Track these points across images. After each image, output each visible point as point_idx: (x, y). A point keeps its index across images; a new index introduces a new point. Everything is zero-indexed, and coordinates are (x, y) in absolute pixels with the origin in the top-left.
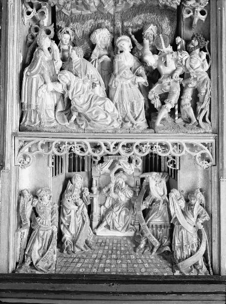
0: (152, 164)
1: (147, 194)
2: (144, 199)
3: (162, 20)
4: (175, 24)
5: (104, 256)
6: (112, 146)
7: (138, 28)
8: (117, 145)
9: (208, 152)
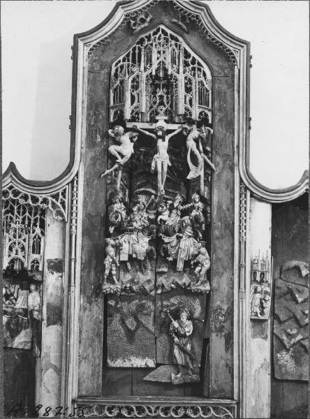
3: (194, 301)
4: (205, 306)
8: (157, 408)
9: (230, 414)
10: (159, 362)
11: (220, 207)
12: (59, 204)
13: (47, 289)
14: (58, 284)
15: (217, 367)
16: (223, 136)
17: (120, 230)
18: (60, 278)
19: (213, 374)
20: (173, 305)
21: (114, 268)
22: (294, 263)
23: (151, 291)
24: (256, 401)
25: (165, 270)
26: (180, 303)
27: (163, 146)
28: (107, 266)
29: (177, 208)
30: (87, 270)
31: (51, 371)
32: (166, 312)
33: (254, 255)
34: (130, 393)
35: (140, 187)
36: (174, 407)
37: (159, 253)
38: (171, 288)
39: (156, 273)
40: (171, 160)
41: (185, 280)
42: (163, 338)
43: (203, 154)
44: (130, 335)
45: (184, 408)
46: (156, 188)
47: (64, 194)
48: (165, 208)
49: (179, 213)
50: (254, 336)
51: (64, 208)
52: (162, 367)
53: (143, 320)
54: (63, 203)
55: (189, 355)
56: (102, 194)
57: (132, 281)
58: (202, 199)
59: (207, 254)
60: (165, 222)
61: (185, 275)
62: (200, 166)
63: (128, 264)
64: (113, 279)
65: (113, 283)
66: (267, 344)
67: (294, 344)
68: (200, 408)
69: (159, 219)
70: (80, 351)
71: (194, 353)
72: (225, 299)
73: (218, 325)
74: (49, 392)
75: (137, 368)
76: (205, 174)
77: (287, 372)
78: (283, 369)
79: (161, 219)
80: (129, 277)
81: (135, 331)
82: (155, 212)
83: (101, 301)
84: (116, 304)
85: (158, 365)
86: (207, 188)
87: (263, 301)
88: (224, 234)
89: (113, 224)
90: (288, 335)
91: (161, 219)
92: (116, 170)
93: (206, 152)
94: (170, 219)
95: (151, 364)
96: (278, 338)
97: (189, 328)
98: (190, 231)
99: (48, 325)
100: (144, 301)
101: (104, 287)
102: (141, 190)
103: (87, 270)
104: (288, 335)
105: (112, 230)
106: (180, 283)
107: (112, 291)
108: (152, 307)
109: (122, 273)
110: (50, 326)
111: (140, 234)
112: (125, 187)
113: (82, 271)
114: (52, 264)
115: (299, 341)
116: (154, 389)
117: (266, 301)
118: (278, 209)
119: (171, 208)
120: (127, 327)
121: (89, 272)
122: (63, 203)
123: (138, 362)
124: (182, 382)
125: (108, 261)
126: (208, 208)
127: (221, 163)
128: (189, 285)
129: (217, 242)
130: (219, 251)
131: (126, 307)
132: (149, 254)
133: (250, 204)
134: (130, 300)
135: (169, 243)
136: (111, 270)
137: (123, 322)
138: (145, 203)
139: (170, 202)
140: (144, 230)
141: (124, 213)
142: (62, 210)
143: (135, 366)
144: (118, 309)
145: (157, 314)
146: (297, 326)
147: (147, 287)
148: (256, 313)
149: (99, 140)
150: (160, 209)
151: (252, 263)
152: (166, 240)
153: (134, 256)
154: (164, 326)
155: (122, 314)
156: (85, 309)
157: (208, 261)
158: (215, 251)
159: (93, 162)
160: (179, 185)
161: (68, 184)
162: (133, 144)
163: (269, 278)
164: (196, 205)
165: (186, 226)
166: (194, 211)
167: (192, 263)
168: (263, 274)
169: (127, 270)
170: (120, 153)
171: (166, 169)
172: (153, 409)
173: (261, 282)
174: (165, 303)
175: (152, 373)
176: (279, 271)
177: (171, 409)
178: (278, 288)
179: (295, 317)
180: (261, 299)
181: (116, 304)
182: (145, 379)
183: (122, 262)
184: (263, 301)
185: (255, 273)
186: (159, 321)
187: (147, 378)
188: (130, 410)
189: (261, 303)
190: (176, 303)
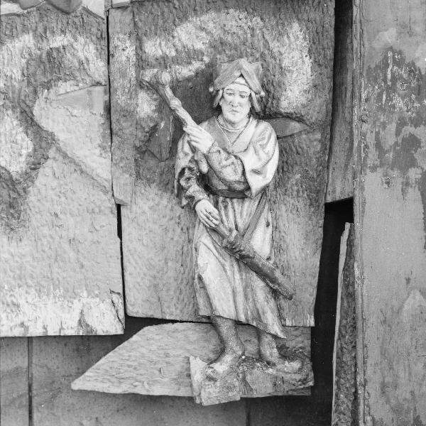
7: (197, 65)
10: (137, 311)
19: (374, 355)
20: (192, 55)
26: (218, 46)
32: (154, 87)
42: (150, 208)
52: (149, 331)
53: (50, 116)
85: (133, 324)
95: (108, 324)
97: (255, 152)
108: (98, 68)
123: (55, 317)
124: (236, 395)
143: (36, 331)
145: (120, 99)
154: (154, 153)
174: (153, 48)
186: (126, 127)
190: (199, 46)
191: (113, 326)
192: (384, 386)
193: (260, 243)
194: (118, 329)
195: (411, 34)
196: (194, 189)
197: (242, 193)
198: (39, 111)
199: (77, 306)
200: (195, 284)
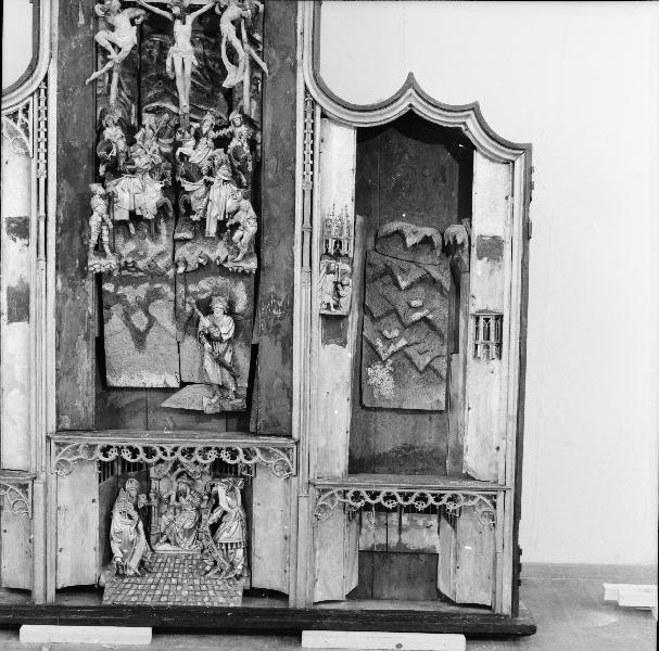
0: (220, 469)
1: (216, 505)
2: (212, 512)
5: (162, 581)
6: (169, 451)
8: (175, 449)
9: (287, 459)
10: (185, 380)
11: (275, 135)
12: (18, 127)
13: (7, 265)
14: (23, 257)
15: (269, 388)
16: (281, 15)
17: (115, 171)
18: (26, 248)
20: (204, 291)
21: (105, 232)
22: (396, 226)
23: (167, 269)
24: (327, 439)
25: (189, 235)
27: (183, 31)
28: (94, 229)
29: (206, 135)
30: (67, 235)
31: (16, 391)
33: (327, 212)
34: (143, 425)
35: (152, 100)
36: (200, 447)
37: (177, 207)
38: (200, 265)
39: (175, 241)
40: (197, 55)
41: (220, 252)
42: (190, 343)
43: (247, 46)
44: (140, 338)
45: (217, 449)
46: (176, 102)
47: (25, 111)
48: (187, 135)
49: (210, 142)
50: (326, 341)
51: (28, 136)
54: (25, 127)
55: (229, 369)
56: (90, 111)
57: (134, 253)
58: (247, 120)
59: (251, 211)
60: (188, 157)
61: (221, 244)
62: (241, 65)
63: (131, 226)
64: (104, 251)
65: (105, 256)
66: (347, 354)
67: (393, 353)
68: (241, 451)
69: (178, 154)
70: (59, 363)
71: (237, 368)
72: (282, 282)
73: (271, 324)
74: (14, 423)
75: (152, 389)
76: (253, 80)
77: (381, 396)
78: (376, 391)
79: (181, 153)
80: (131, 246)
81: (147, 331)
82: (171, 141)
83: (90, 285)
84: (116, 289)
85: (183, 384)
86: (254, 103)
87: (339, 286)
88: (281, 177)
89: (105, 161)
90: (385, 339)
91: (181, 153)
92: (110, 72)
93: (253, 42)
94: (198, 153)
95: (174, 383)
96: (370, 344)
97: (226, 327)
98: (226, 172)
99: (11, 320)
100: (158, 286)
101: (90, 263)
102: (154, 105)
103: (67, 235)
104: (385, 339)
105: (102, 169)
106: (213, 257)
107: (103, 270)
108: (171, 295)
109: (120, 240)
110: (13, 324)
111: (148, 176)
112: (129, 102)
113: (58, 235)
114: (13, 225)
115: (401, 350)
116: (181, 420)
117: (342, 285)
118: (364, 136)
119: (198, 136)
120: (133, 325)
121: (72, 237)
122: (25, 127)
123: (155, 381)
124: (218, 410)
125: (94, 221)
126: (258, 136)
127: (278, 61)
128: (226, 261)
129: (270, 191)
130: (274, 206)
131: (132, 294)
132: (162, 209)
133: (322, 129)
134: (136, 282)
135: (193, 192)
136: (100, 239)
137: (127, 317)
138: (154, 126)
139: (196, 125)
140: (153, 170)
141: (122, 144)
142: (25, 138)
143: (148, 385)
144: (118, 297)
145: (180, 306)
146: (399, 325)
147: (161, 263)
148: (328, 304)
149: (82, 21)
150: (179, 136)
151: (326, 224)
152: (188, 186)
153: (138, 213)
154: (189, 325)
155: (126, 304)
156: (65, 297)
157: (252, 221)
158: (267, 206)
159: (72, 58)
160: (217, 98)
161: (32, 95)
162: (135, 28)
163: (351, 249)
164: (238, 130)
165: (220, 165)
166: (234, 140)
167: (228, 224)
168: (338, 243)
169: (129, 237)
170: (114, 45)
171: (188, 70)
172: (169, 451)
173: (337, 256)
174: (192, 288)
175: (175, 396)
176: (373, 238)
177: (196, 452)
178: (370, 264)
179: (395, 311)
180: (336, 283)
181: (116, 289)
182: (163, 405)
183: (123, 223)
184: (339, 286)
185: (327, 242)
187: (170, 402)
188: (135, 452)
189: (336, 289)
191: (177, 385)
192: (267, 410)
193: (228, 358)
194: (177, 385)
195: (280, 288)
196: (204, 339)
197: (220, 340)
198: (150, 311)
199: (163, 377)
200: (203, 372)
